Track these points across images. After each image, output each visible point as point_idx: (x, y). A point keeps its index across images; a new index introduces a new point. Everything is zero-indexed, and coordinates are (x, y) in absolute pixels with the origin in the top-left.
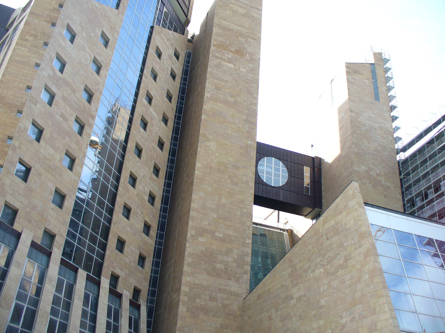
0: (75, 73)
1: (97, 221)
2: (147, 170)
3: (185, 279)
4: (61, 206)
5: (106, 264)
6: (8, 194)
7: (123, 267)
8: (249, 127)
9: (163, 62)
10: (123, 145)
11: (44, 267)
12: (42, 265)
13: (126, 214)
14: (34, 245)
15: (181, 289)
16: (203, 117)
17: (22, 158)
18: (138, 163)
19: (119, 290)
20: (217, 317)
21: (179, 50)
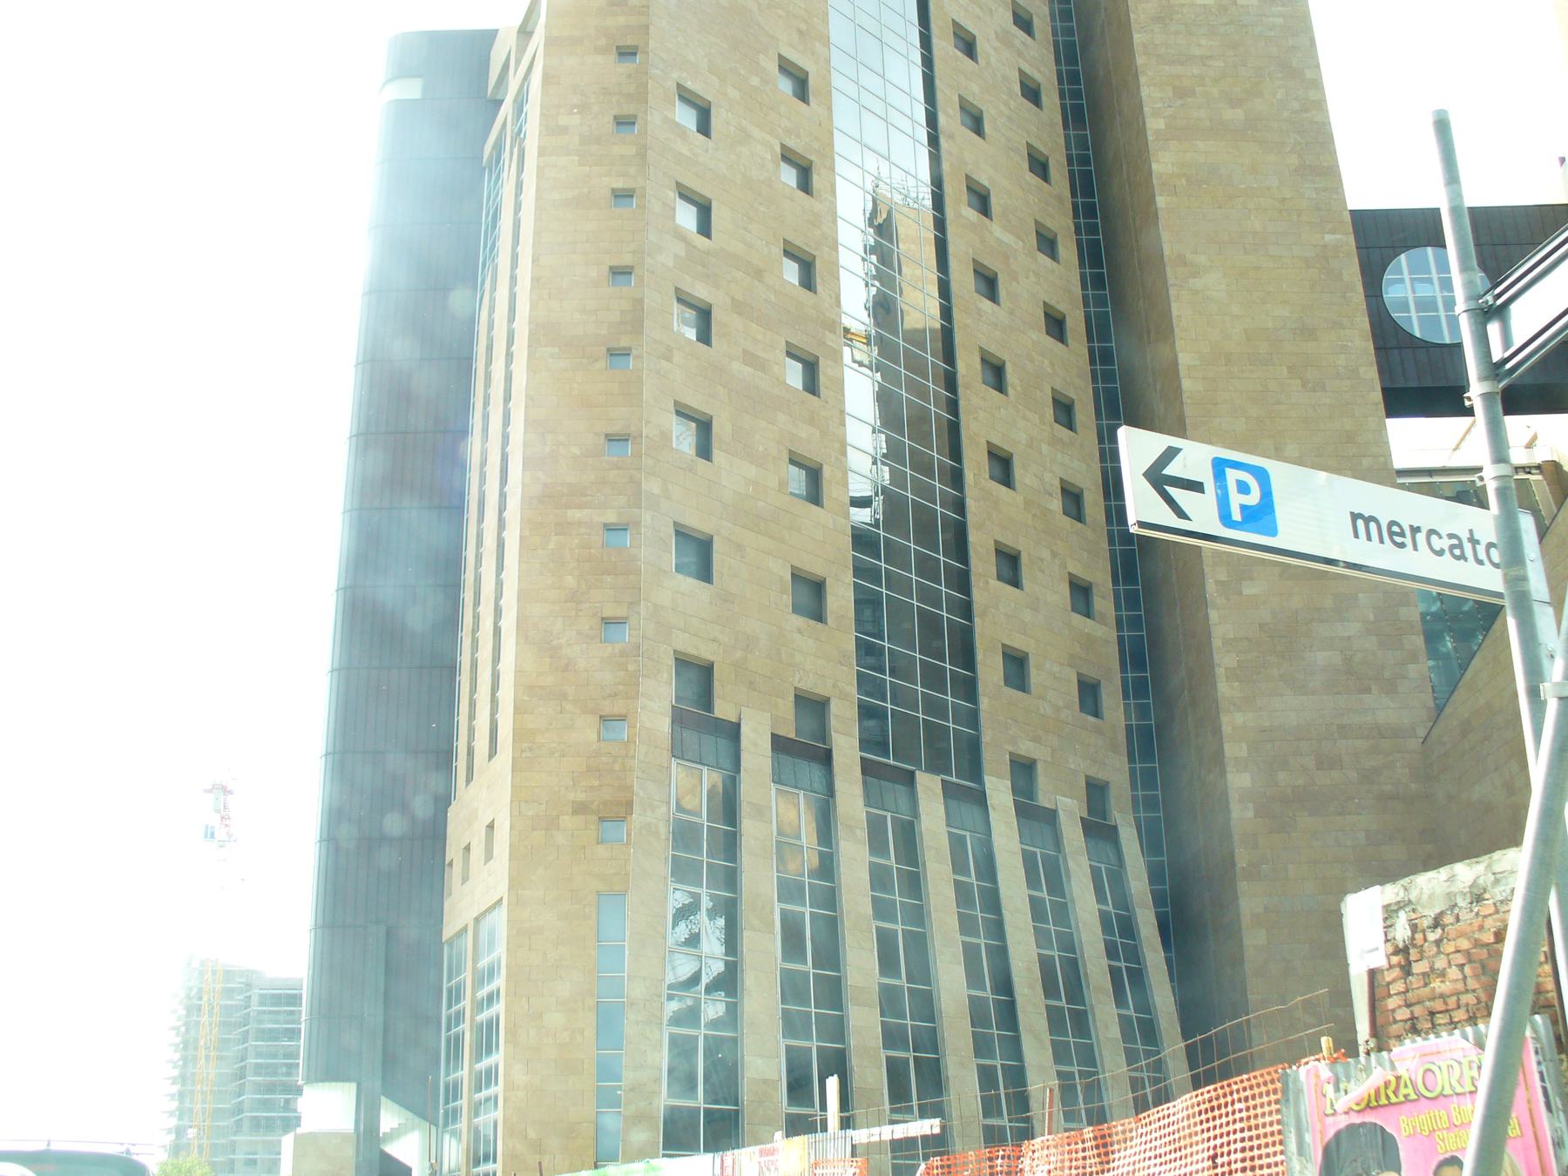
0: (745, 218)
1: (931, 624)
2: (1035, 418)
3: (1233, 721)
4: (819, 615)
5: (987, 737)
6: (674, 630)
7: (1040, 732)
8: (1316, 189)
9: (988, 63)
10: (942, 370)
11: (823, 795)
12: (815, 792)
13: (1007, 572)
15: (1223, 755)
16: (1161, 201)
17: (681, 520)
18: (1002, 409)
19: (1044, 800)
20: (1350, 814)
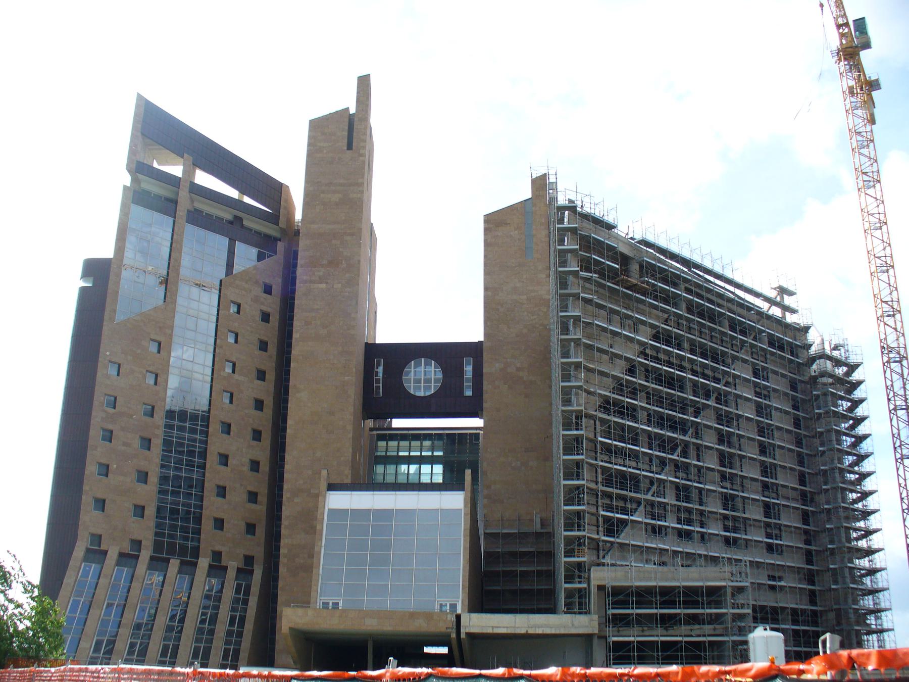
14: (122, 555)
21: (267, 281)
